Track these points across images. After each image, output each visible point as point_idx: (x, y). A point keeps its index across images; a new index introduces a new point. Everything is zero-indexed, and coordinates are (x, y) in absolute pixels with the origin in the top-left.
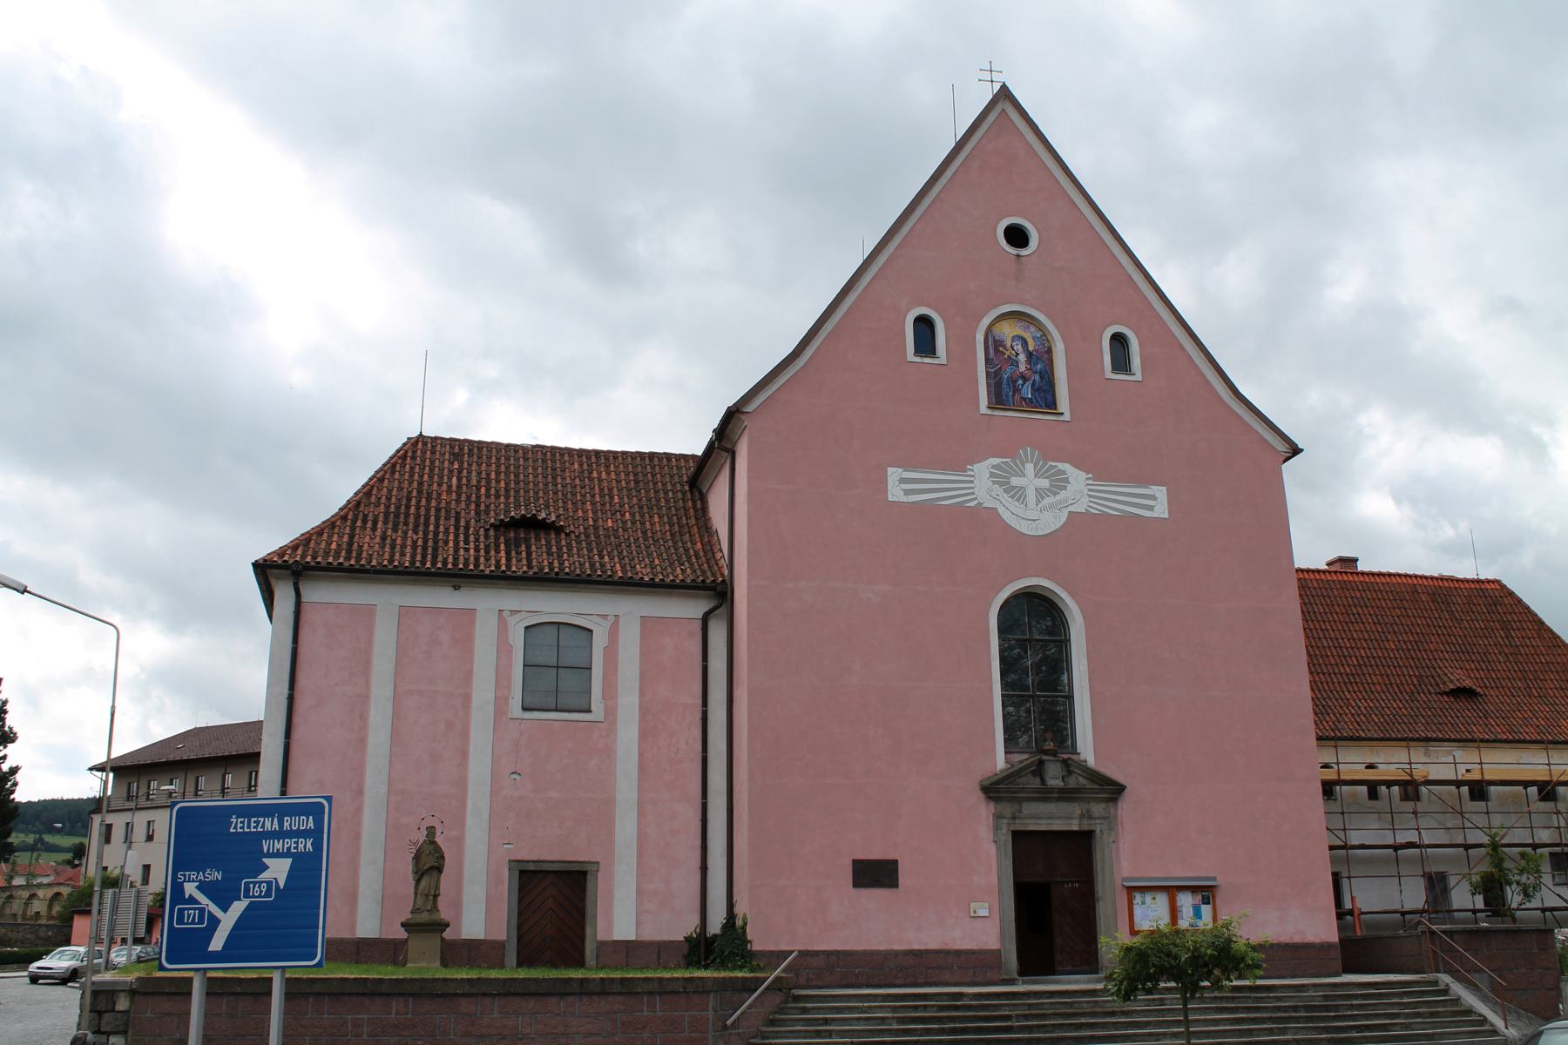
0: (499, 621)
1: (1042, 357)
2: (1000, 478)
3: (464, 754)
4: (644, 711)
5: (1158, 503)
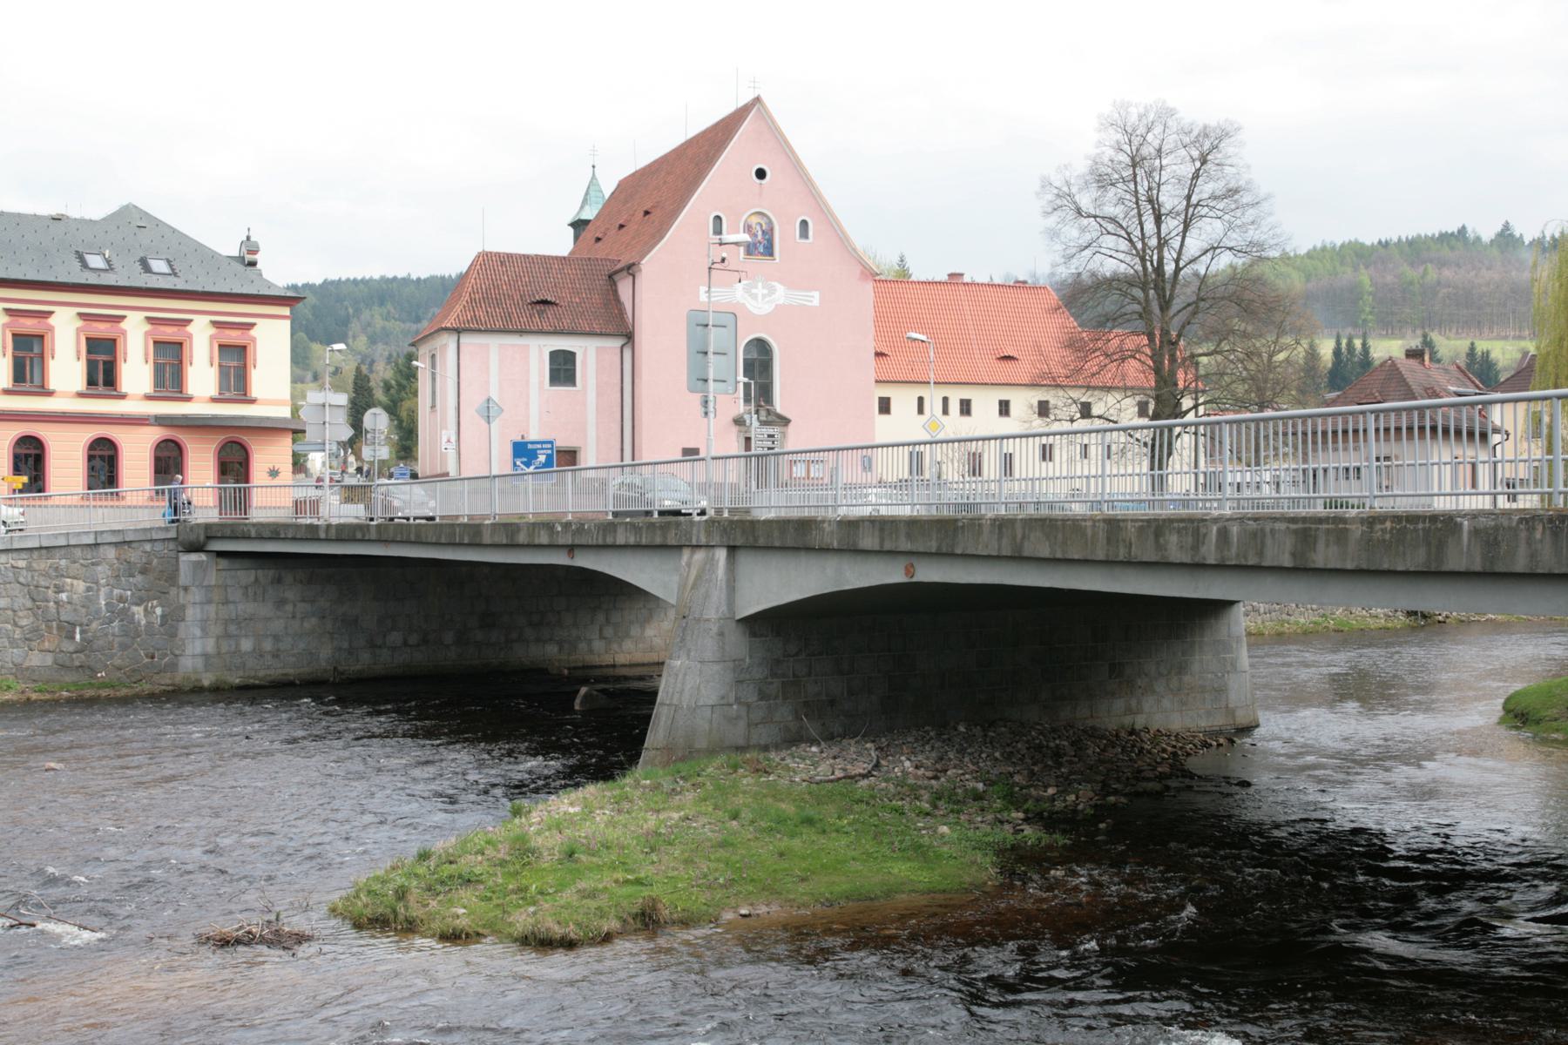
0: (539, 350)
1: (769, 233)
2: (747, 290)
3: (527, 404)
4: (598, 386)
5: (815, 299)
